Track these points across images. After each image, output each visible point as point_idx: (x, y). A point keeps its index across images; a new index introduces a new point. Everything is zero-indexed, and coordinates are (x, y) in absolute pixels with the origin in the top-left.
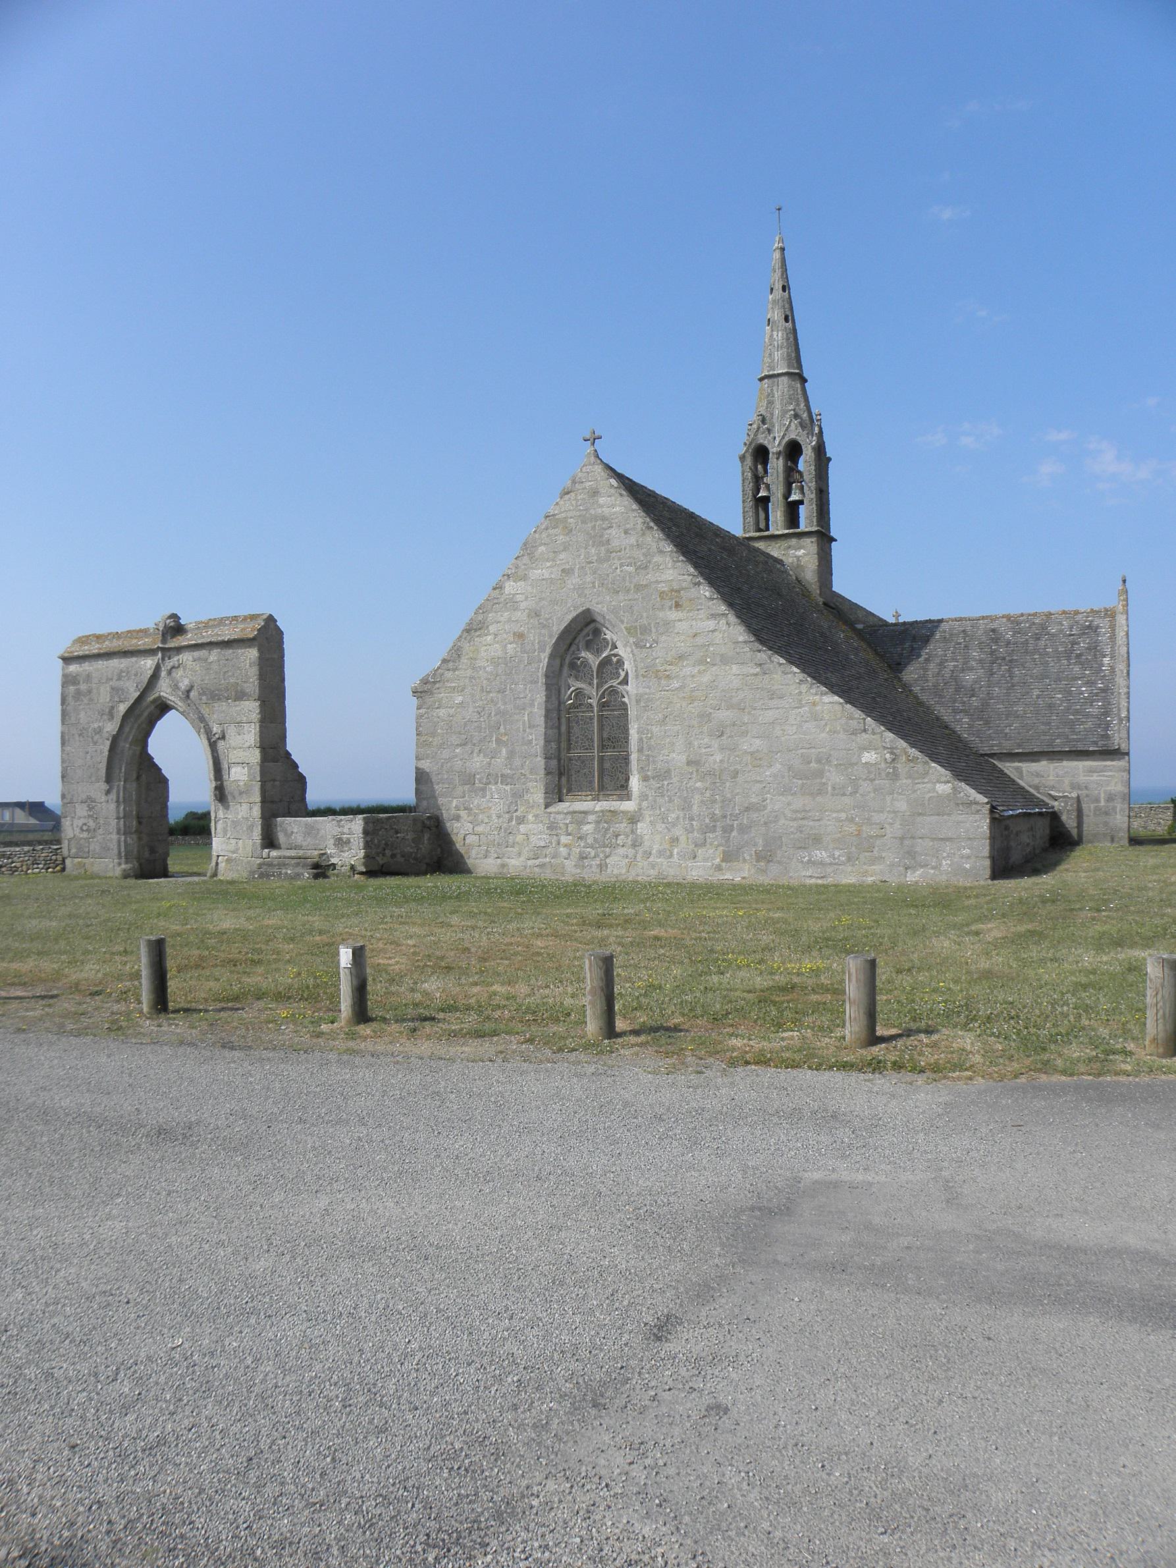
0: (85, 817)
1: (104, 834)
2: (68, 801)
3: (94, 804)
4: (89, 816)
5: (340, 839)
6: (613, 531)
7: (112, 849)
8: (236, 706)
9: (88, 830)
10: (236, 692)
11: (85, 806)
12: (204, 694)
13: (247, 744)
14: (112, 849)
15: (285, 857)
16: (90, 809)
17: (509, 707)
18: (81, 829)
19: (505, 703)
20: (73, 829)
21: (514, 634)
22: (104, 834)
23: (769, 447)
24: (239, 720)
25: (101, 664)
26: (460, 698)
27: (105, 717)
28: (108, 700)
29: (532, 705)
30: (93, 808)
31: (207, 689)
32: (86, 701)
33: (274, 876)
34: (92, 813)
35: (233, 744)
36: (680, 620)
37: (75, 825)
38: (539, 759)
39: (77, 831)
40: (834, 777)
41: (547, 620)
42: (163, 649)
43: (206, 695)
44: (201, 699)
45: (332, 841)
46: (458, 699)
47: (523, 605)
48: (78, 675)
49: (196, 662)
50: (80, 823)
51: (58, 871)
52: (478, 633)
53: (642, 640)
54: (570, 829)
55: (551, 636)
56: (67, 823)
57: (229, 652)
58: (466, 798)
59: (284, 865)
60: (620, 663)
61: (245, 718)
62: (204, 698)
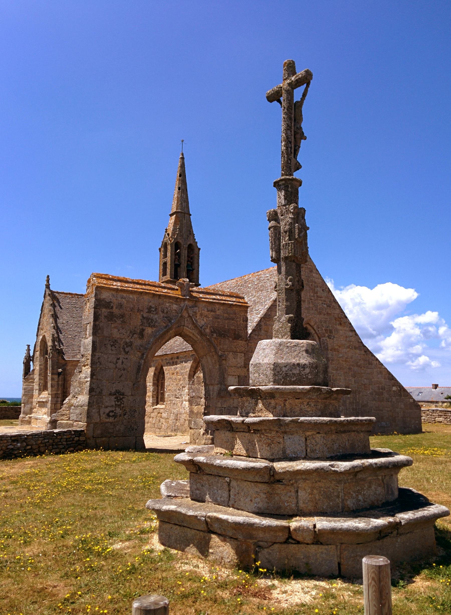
0: (112, 406)
3: (121, 397)
6: (318, 288)
8: (234, 342)
9: (115, 416)
10: (235, 334)
11: (113, 398)
12: (214, 332)
13: (239, 365)
18: (108, 415)
20: (100, 415)
24: (235, 350)
28: (139, 324)
30: (121, 399)
34: (119, 403)
36: (341, 330)
37: (102, 412)
39: (103, 417)
40: (386, 395)
43: (216, 333)
48: (111, 302)
50: (107, 410)
53: (330, 336)
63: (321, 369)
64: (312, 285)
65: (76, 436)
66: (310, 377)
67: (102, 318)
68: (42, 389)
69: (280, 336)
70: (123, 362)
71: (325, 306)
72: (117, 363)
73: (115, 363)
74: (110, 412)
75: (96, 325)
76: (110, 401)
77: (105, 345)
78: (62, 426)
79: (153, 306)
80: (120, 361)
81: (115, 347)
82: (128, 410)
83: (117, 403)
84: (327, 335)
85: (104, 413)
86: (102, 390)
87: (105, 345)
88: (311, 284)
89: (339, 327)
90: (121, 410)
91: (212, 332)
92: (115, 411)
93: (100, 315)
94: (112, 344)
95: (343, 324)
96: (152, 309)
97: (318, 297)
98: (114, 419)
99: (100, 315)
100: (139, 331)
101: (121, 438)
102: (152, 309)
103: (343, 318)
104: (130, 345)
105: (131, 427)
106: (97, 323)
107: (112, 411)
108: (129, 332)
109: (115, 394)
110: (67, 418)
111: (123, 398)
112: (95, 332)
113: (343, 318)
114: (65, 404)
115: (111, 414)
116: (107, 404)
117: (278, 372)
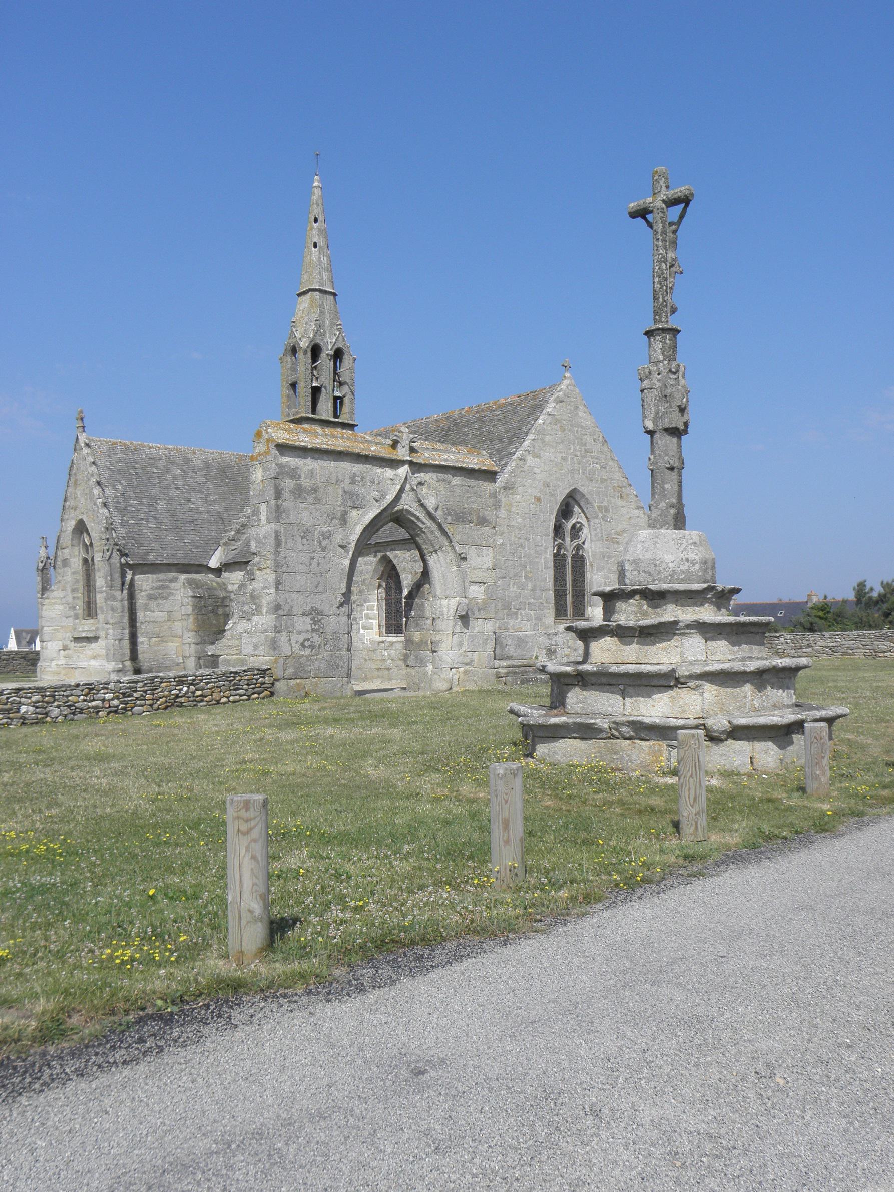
1: (331, 651)
2: (285, 613)
3: (320, 617)
4: (313, 630)
5: (550, 650)
7: (342, 667)
9: (312, 647)
10: (478, 517)
11: (308, 620)
12: (449, 514)
13: (485, 566)
14: (342, 667)
15: (514, 666)
16: (315, 623)
17: (532, 552)
18: (303, 645)
19: (529, 549)
20: (291, 645)
21: (535, 497)
22: (331, 651)
23: (324, 348)
25: (331, 465)
26: (501, 541)
27: (335, 521)
28: (339, 503)
29: (546, 552)
30: (319, 621)
31: (452, 510)
32: (311, 500)
33: (532, 681)
34: (317, 627)
35: (474, 565)
37: (293, 642)
38: (551, 592)
39: (296, 648)
41: (554, 490)
42: (411, 463)
44: (446, 519)
45: (544, 652)
46: (500, 542)
47: (539, 477)
48: (297, 468)
49: (441, 482)
50: (301, 639)
51: (266, 697)
52: (511, 492)
54: (569, 644)
55: (556, 503)
56: (282, 639)
57: (472, 482)
58: (505, 620)
59: (526, 672)
60: (580, 529)
61: (484, 542)
62: (449, 518)
63: (710, 564)
64: (577, 431)
65: (261, 677)
66: (700, 574)
67: (286, 494)
68: (80, 616)
69: (658, 526)
70: (319, 564)
71: (598, 466)
72: (311, 564)
73: (308, 564)
74: (305, 640)
75: (278, 506)
76: (303, 624)
77: (293, 536)
78: (228, 662)
79: (358, 473)
80: (314, 562)
81: (308, 540)
82: (329, 637)
83: (313, 627)
84: (600, 515)
85: (297, 642)
86: (292, 607)
87: (293, 536)
88: (575, 429)
89: (620, 502)
90: (319, 637)
91: (445, 514)
92: (311, 640)
93: (282, 489)
94: (302, 534)
95: (625, 497)
96: (357, 478)
97: (586, 451)
98: (312, 651)
99: (282, 489)
100: (339, 514)
101: (322, 680)
102: (357, 478)
103: (625, 487)
104: (328, 536)
105: (335, 663)
106: (280, 502)
107: (308, 640)
108: (326, 515)
109: (311, 614)
110: (237, 652)
111: (322, 618)
112: (278, 516)
113: (625, 487)
114: (228, 630)
115: (307, 644)
116: (301, 628)
117: (664, 569)
